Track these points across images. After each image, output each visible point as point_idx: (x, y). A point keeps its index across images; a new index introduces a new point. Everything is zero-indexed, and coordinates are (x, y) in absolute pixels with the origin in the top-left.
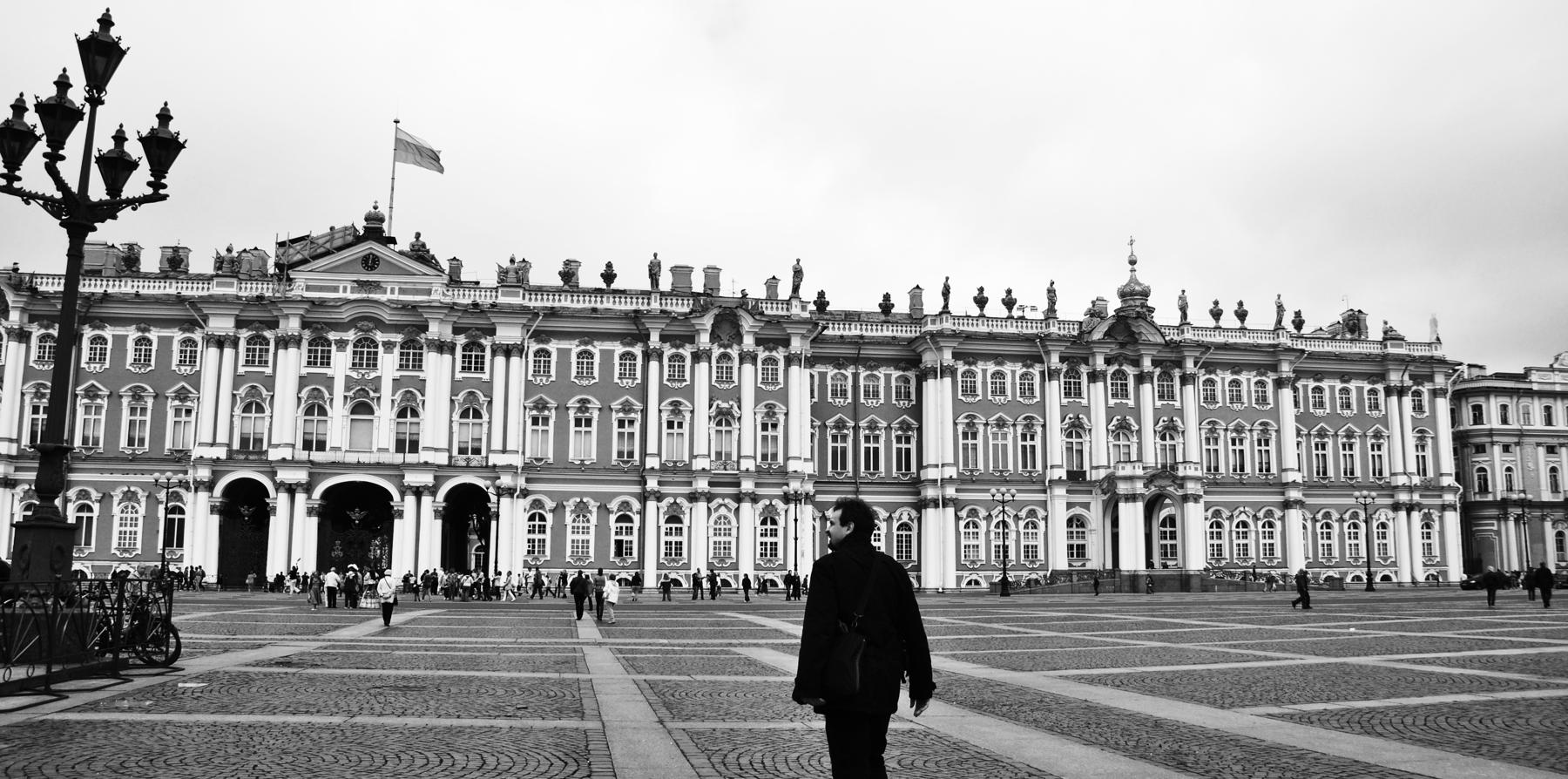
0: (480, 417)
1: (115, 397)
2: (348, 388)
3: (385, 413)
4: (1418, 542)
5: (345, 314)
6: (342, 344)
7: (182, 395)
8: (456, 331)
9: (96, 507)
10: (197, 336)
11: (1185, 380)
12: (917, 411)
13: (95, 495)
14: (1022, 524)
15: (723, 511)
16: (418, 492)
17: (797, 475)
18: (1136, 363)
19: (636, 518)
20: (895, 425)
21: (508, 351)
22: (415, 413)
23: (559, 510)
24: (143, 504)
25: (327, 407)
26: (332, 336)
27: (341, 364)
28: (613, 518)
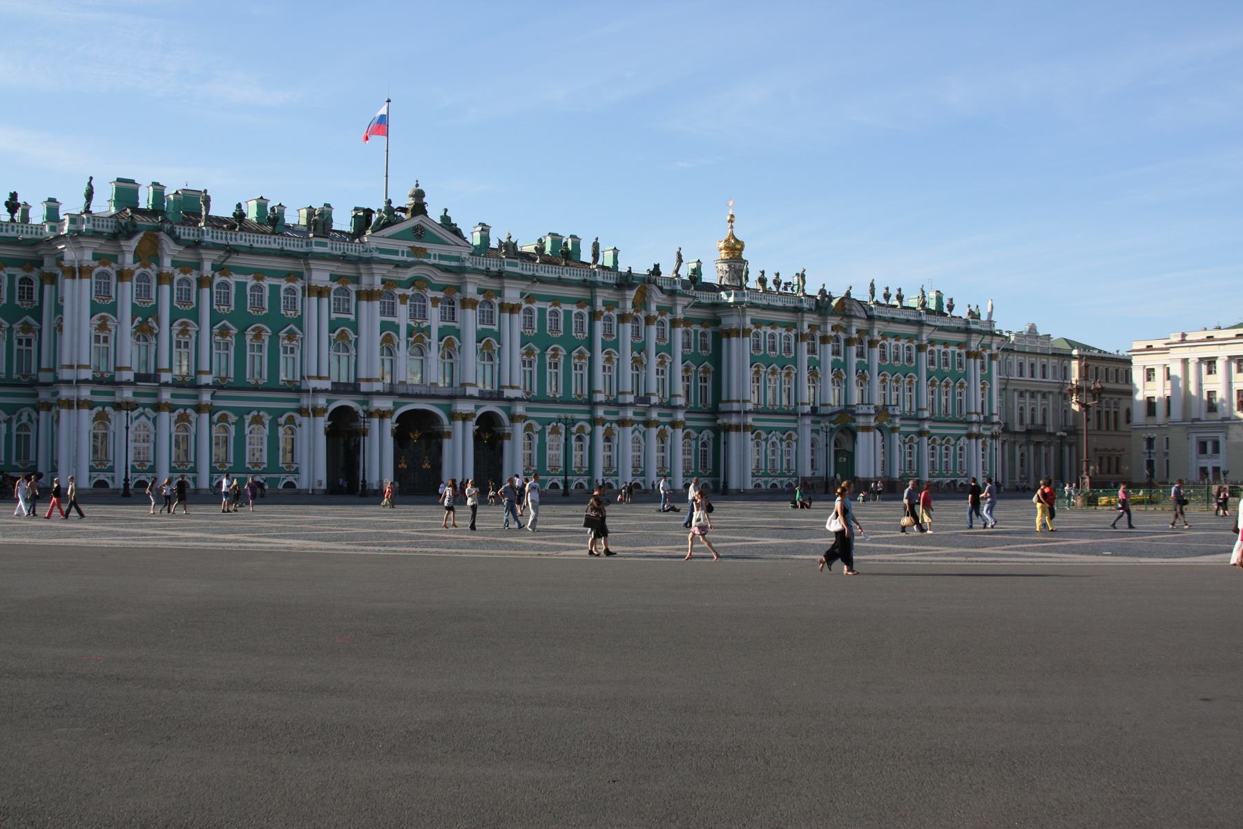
2: (410, 334)
3: (434, 354)
4: (981, 460)
5: (409, 274)
6: (404, 298)
7: (291, 336)
8: (481, 291)
9: (232, 429)
10: (298, 286)
11: (872, 344)
12: (717, 358)
13: (233, 418)
14: (784, 444)
15: (637, 433)
16: (465, 418)
17: (680, 407)
18: (845, 331)
19: (587, 438)
20: (700, 369)
21: (513, 309)
22: (450, 357)
23: (542, 434)
26: (399, 291)
27: (403, 315)
28: (574, 437)
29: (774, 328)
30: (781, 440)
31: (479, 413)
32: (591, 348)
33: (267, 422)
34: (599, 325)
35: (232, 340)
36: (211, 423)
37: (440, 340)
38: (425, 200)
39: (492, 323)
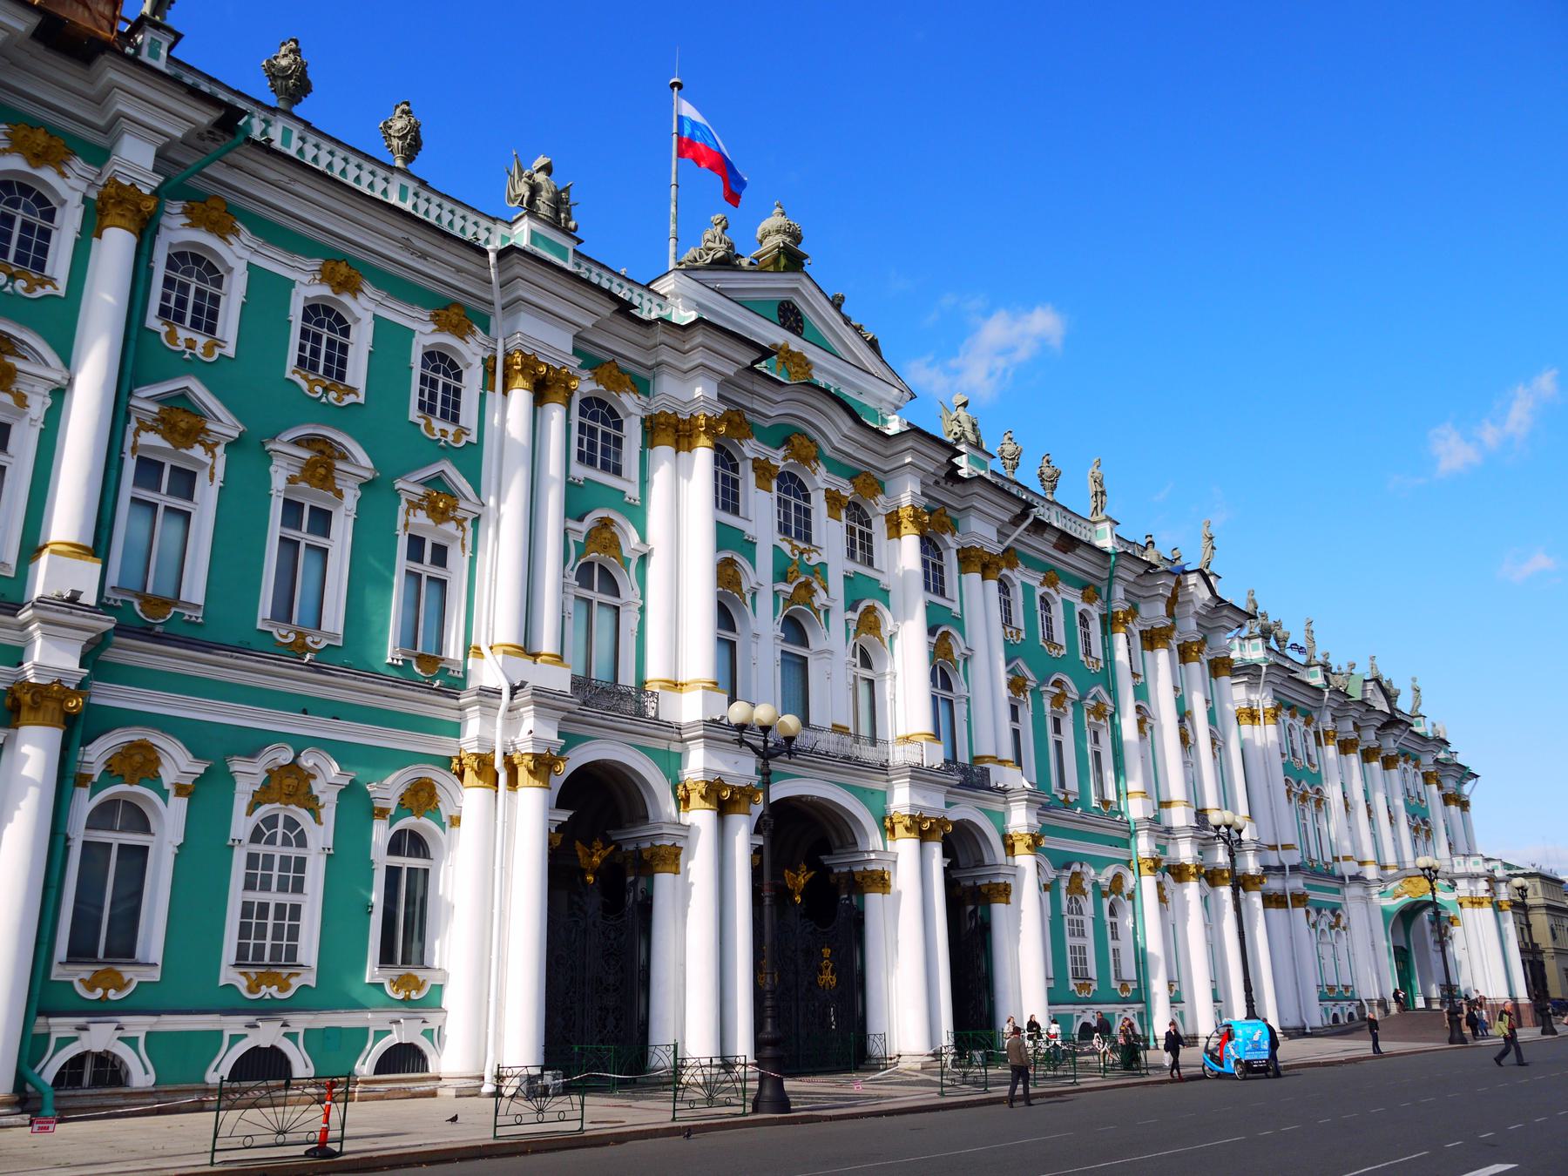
0: (950, 689)
1: (249, 451)
2: (782, 575)
6: (763, 470)
10: (470, 352)
13: (178, 763)
24: (329, 814)
25: (749, 610)
26: (751, 449)
28: (1106, 903)
29: (1293, 716)
30: (1331, 927)
31: (955, 815)
32: (1113, 692)
33: (329, 802)
34: (1120, 640)
35: (213, 472)
36: (67, 777)
37: (852, 607)
38: (801, 248)
39: (942, 594)
